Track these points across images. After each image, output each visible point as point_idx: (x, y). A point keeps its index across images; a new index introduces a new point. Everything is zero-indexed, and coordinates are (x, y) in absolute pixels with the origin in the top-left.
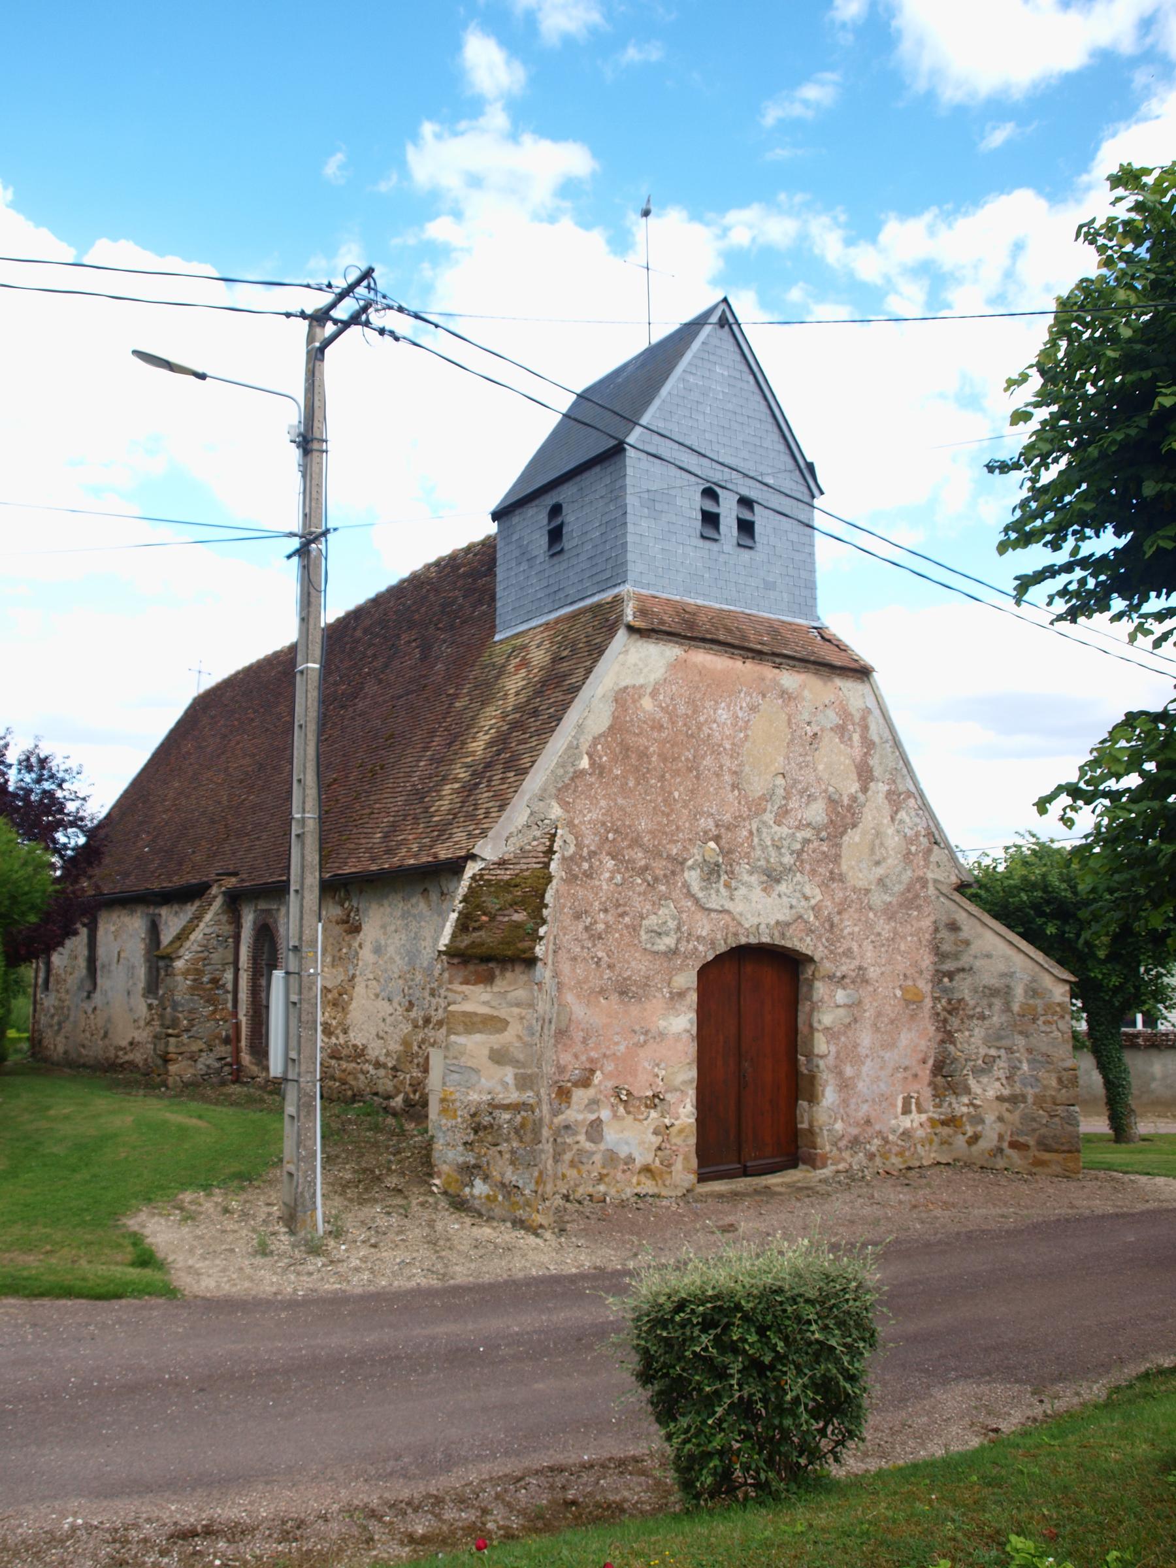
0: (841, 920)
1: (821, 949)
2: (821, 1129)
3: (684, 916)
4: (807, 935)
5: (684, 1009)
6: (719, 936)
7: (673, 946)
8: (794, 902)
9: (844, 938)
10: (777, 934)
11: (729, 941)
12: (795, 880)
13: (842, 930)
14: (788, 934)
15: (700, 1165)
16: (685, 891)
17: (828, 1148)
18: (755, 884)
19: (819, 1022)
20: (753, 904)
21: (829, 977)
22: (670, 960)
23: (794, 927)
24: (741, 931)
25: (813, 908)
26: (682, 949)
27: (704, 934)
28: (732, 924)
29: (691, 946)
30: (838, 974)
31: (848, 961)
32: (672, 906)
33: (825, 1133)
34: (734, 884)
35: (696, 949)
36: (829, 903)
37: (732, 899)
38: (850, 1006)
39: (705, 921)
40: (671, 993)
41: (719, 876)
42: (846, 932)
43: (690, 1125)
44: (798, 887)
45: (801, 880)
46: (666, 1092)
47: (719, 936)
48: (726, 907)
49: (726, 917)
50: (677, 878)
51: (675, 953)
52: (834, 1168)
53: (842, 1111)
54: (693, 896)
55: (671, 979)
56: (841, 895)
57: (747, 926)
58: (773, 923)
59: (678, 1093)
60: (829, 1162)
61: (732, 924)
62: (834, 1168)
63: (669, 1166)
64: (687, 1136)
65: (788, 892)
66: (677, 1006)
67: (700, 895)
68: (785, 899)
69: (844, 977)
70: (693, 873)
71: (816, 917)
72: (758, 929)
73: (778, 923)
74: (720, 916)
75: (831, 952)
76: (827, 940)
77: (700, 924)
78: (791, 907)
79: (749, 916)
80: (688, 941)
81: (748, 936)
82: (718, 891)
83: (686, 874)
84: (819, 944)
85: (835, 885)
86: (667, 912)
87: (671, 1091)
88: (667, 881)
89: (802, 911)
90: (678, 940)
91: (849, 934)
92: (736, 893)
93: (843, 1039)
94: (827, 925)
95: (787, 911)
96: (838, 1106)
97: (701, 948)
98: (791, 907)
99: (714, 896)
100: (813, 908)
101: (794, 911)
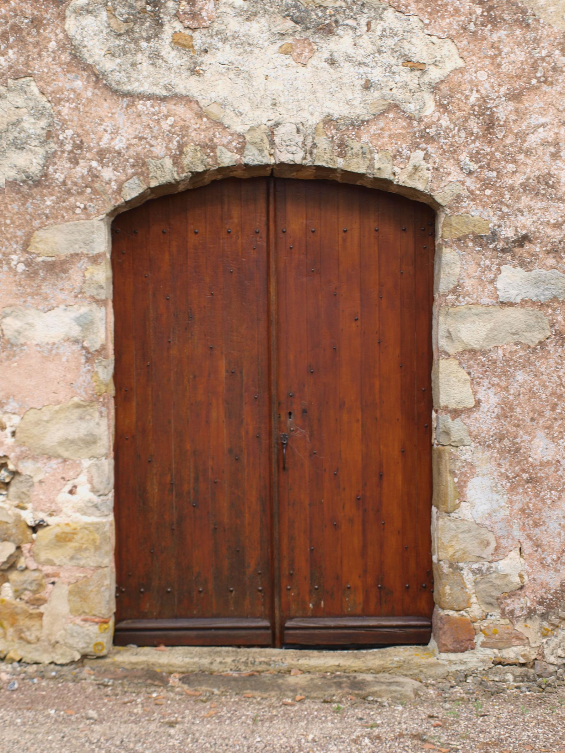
0: (521, 115)
1: (456, 175)
2: (455, 567)
3: (65, 110)
4: (415, 146)
5: (62, 296)
6: (159, 150)
7: (35, 169)
8: (376, 75)
9: (528, 153)
10: (323, 143)
11: (186, 161)
12: (378, 27)
13: (522, 136)
14: (356, 146)
15: (119, 616)
16: (65, 57)
17: (476, 610)
18: (262, 39)
19: (449, 336)
20: (259, 82)
21: (478, 239)
22: (25, 198)
23: (373, 129)
24: (221, 138)
25: (435, 88)
26: (60, 176)
27: (119, 144)
28: (193, 123)
29: (81, 170)
30: (508, 232)
31: (539, 204)
32: (34, 88)
33: (468, 577)
34: (199, 39)
35: (95, 176)
36: (482, 76)
37: (194, 71)
38: (543, 306)
39: (121, 119)
40: (28, 264)
41: (159, 24)
42: (533, 140)
43: (97, 527)
44: (391, 42)
45: (398, 26)
46: (22, 457)
47: (159, 150)
48: (180, 89)
49: (181, 110)
50: (47, 33)
51: (37, 184)
52: (490, 653)
53: (517, 533)
54: (88, 68)
55: (29, 236)
56: (520, 55)
57: (239, 128)
58: (315, 119)
59: (54, 463)
60: (480, 639)
61: (193, 123)
62: (490, 653)
63: (38, 602)
64: (79, 550)
65: (359, 54)
66: (46, 289)
67: (108, 65)
68: (347, 69)
69: (523, 240)
70: (88, 20)
71: (442, 107)
72: (271, 134)
73: (329, 121)
74: (164, 108)
75: (486, 184)
76: (475, 157)
77: (108, 124)
78: (367, 86)
79: (245, 107)
80: (75, 162)
81: (241, 150)
82: (156, 56)
83: (71, 25)
84: (450, 166)
85: (502, 33)
86: (20, 101)
87: (34, 458)
88: (21, 40)
89: (399, 95)
90: (49, 158)
91: (545, 143)
92: (206, 58)
93: (520, 376)
94: (474, 125)
95: (358, 94)
96: (508, 521)
97: (107, 173)
98: (367, 86)
99: (145, 67)
100: (435, 88)
101: (375, 94)
